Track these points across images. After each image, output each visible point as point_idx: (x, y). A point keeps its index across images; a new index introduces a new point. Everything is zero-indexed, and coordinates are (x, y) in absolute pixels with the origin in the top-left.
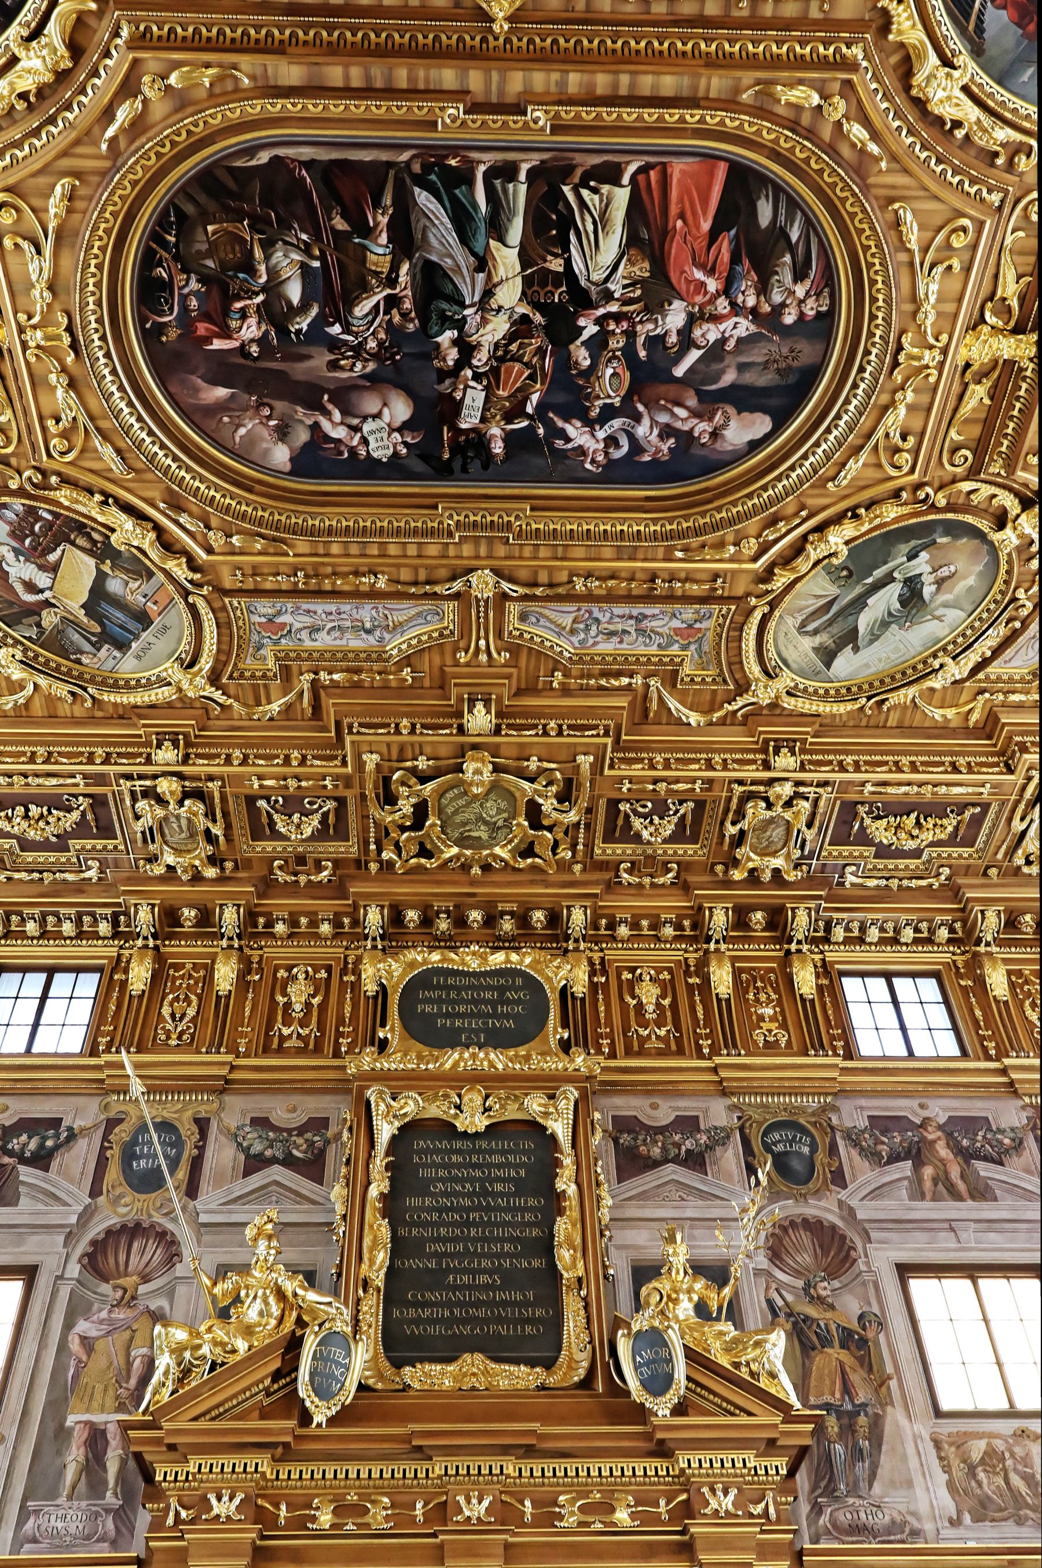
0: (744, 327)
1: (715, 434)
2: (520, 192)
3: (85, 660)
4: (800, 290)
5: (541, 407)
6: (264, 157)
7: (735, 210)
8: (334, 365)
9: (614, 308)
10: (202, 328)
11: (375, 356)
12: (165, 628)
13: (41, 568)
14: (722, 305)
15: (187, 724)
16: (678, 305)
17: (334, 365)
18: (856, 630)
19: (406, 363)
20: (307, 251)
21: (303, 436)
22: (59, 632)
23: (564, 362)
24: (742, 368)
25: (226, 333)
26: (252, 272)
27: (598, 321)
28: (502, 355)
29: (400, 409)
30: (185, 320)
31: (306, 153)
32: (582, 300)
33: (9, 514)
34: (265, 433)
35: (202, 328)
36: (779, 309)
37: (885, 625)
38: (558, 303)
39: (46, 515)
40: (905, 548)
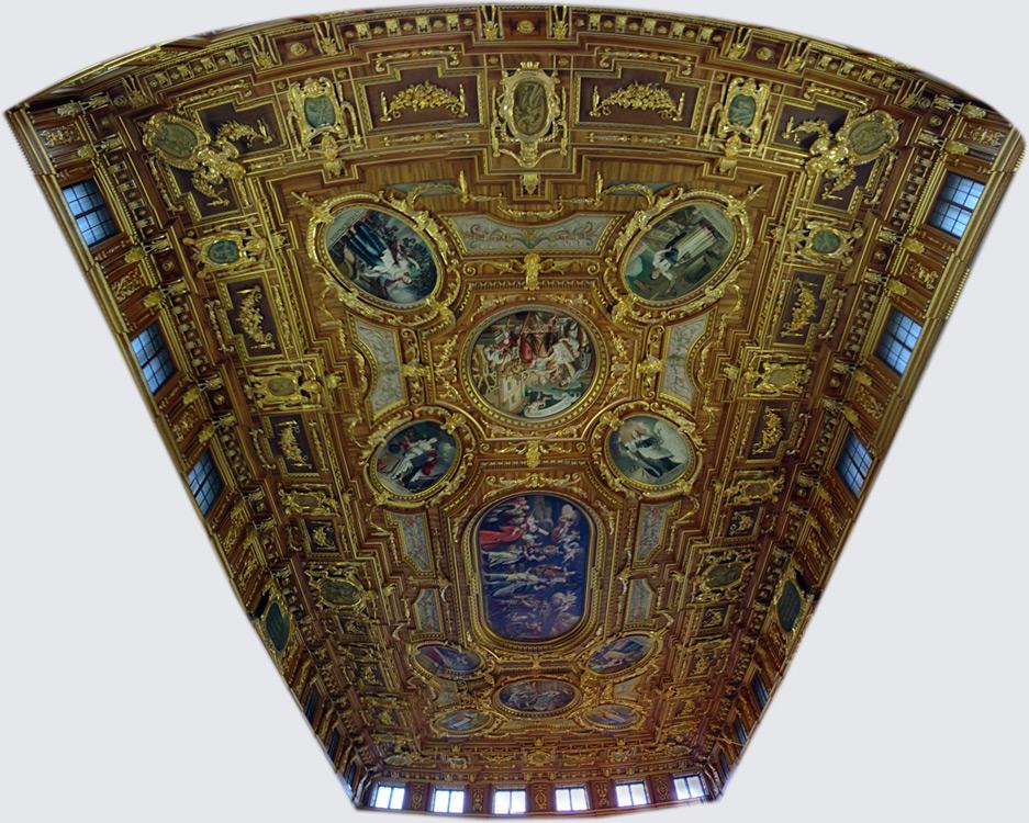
0: (531, 520)
1: (571, 520)
2: (492, 575)
4: (517, 506)
7: (494, 527)
9: (525, 552)
14: (524, 526)
15: (671, 640)
16: (524, 537)
18: (662, 459)
19: (547, 594)
21: (568, 614)
23: (544, 561)
24: (545, 517)
26: (518, 625)
27: (530, 555)
28: (543, 576)
29: (560, 595)
32: (523, 559)
36: (524, 511)
38: (523, 564)
40: (622, 452)
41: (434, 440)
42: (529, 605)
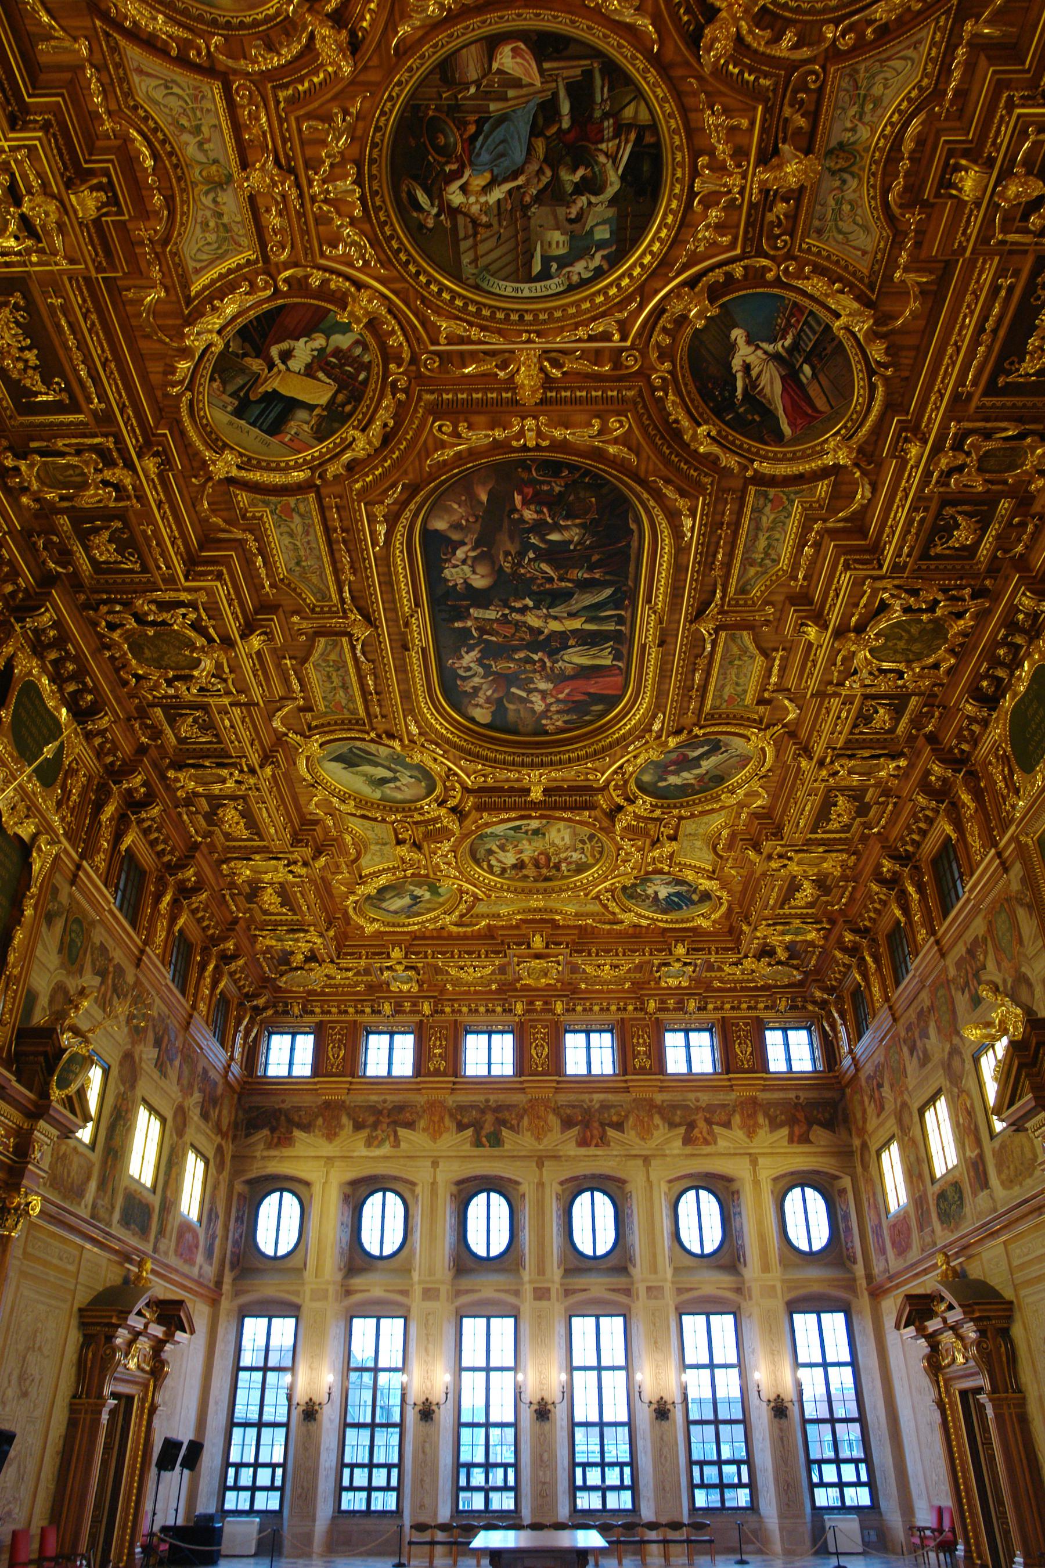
0: (539, 706)
3: (215, 385)
5: (487, 641)
6: (633, 526)
8: (507, 553)
10: (529, 491)
11: (515, 573)
12: (268, 445)
13: (308, 366)
16: (551, 686)
17: (507, 553)
20: (579, 543)
21: (456, 536)
22: (243, 370)
23: (516, 649)
24: (518, 711)
25: (525, 503)
26: (566, 518)
27: (541, 660)
28: (517, 625)
29: (479, 582)
30: (532, 482)
31: (635, 544)
32: (552, 653)
33: (358, 351)
34: (455, 518)
35: (529, 491)
37: (365, 775)
39: (362, 377)
41: (661, 784)
42: (544, 566)
